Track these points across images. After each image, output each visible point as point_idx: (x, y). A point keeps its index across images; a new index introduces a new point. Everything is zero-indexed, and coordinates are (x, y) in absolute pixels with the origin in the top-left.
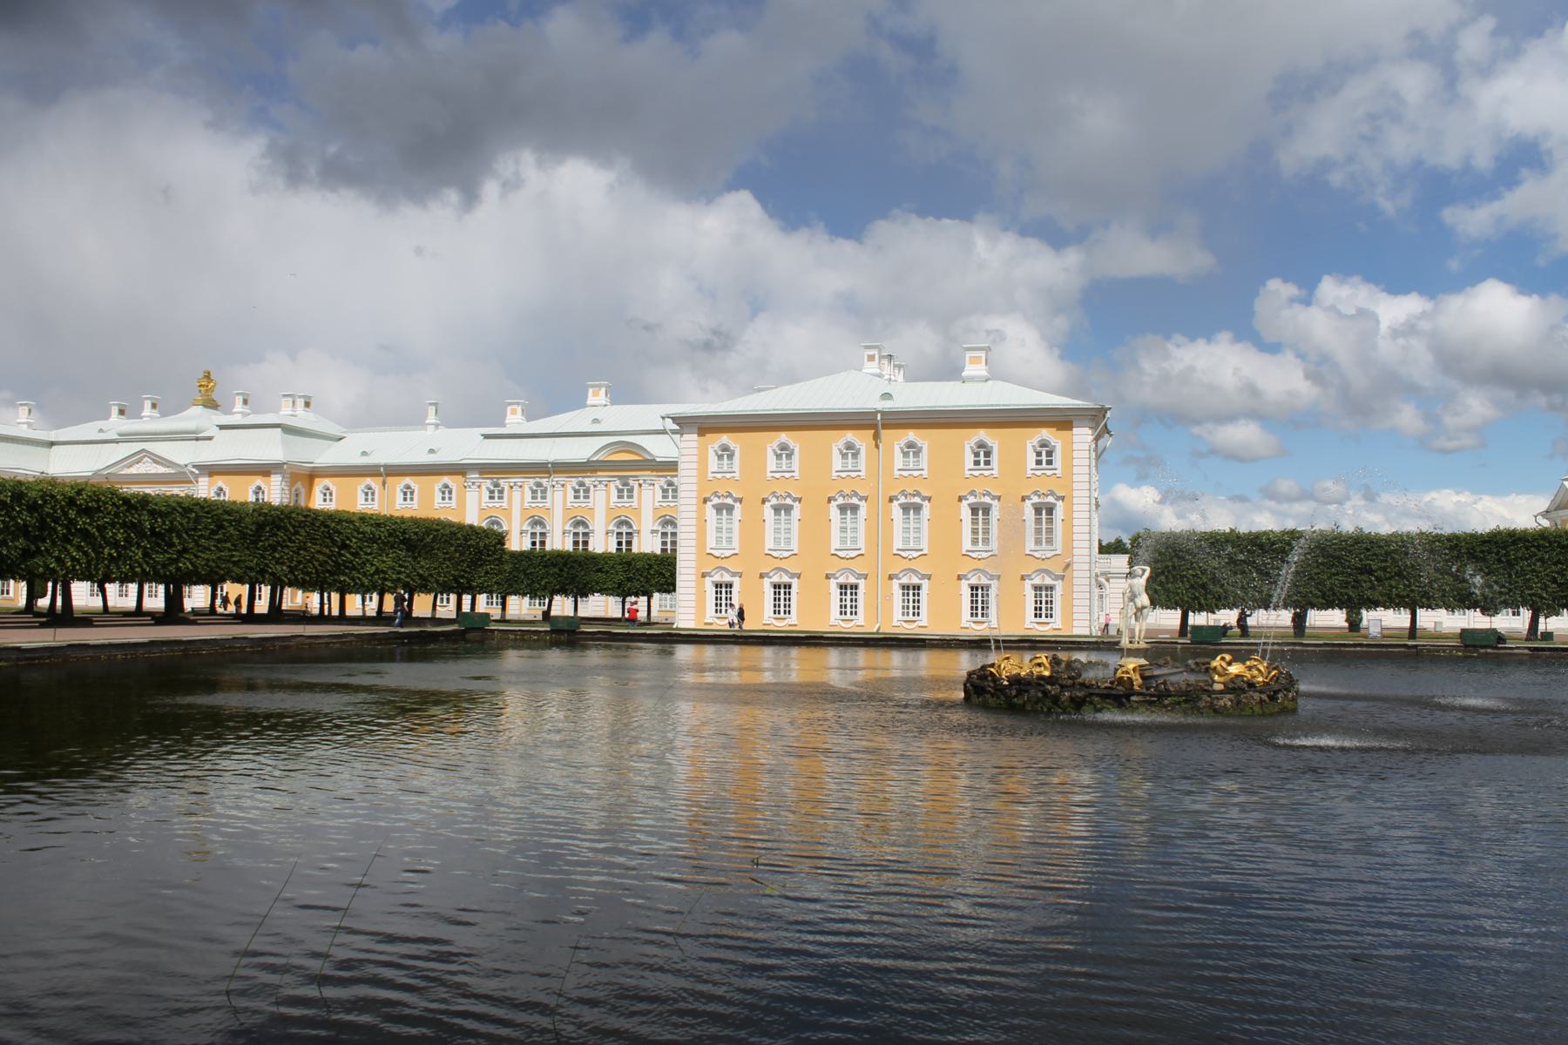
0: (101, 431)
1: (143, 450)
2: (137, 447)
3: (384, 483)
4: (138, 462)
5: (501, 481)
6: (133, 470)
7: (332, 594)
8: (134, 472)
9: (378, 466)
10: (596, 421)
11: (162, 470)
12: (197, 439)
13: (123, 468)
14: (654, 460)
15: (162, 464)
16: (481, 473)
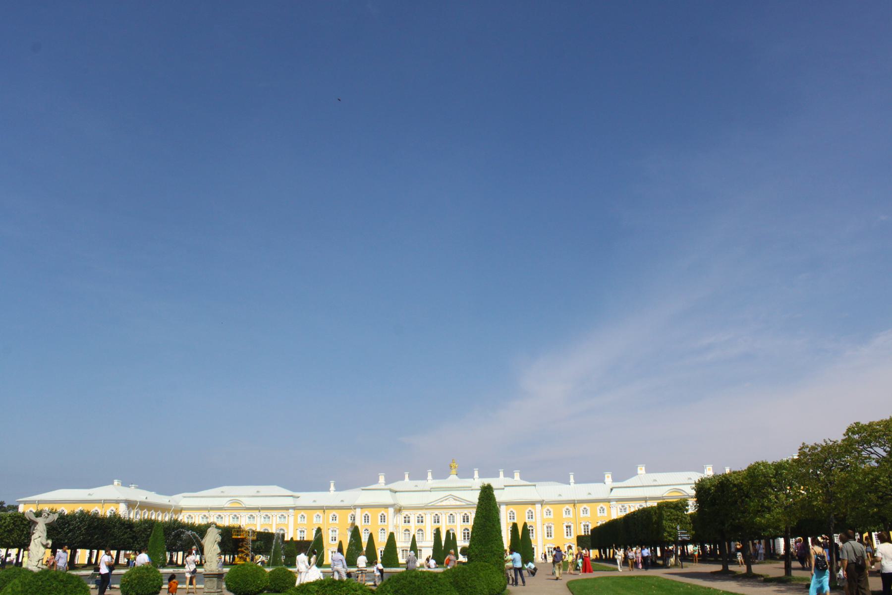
0: (416, 486)
1: (451, 495)
2: (450, 493)
3: (574, 506)
4: (446, 500)
5: (625, 505)
6: (444, 503)
7: (228, 561)
8: (444, 504)
9: (574, 500)
10: (655, 480)
11: (458, 503)
12: (472, 490)
13: (438, 503)
14: (688, 495)
15: (458, 501)
16: (616, 502)
